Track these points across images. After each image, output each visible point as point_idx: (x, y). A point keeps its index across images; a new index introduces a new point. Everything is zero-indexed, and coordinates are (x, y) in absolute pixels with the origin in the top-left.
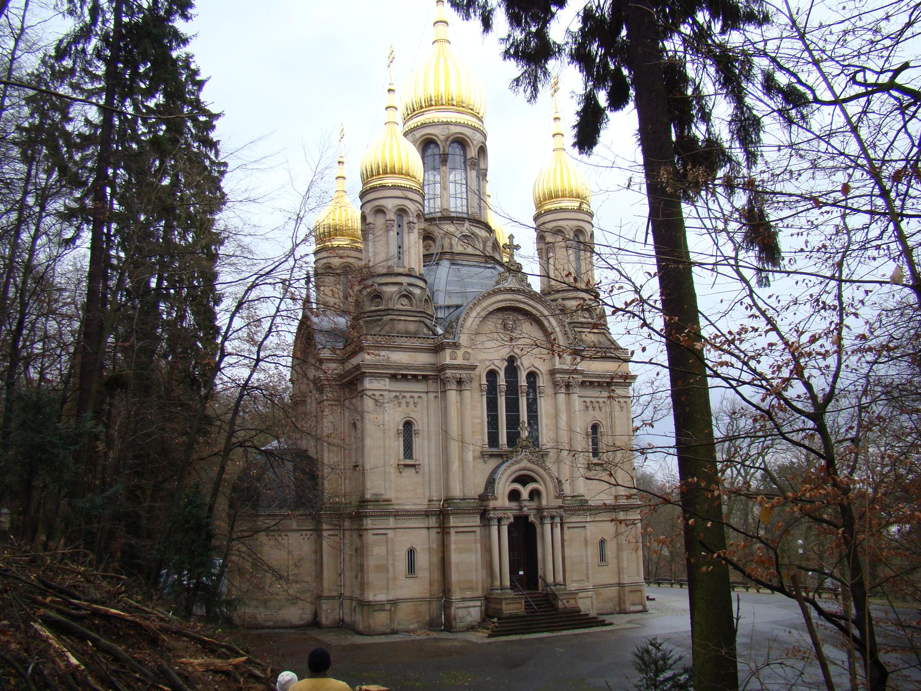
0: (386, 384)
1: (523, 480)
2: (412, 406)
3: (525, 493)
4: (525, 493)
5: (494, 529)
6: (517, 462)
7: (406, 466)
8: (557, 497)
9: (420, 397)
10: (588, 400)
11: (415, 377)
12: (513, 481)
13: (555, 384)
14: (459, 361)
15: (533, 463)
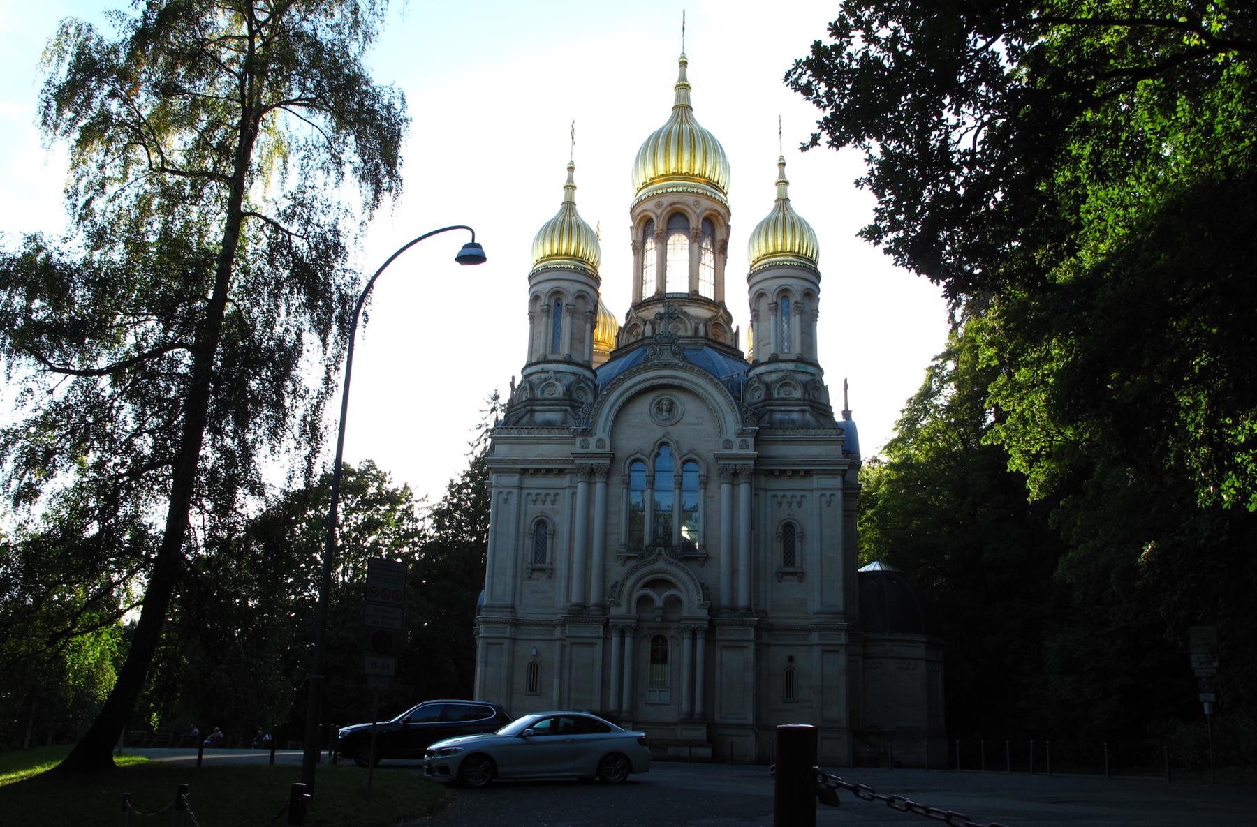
0: (514, 479)
1: (658, 583)
2: (548, 505)
3: (659, 602)
4: (659, 602)
5: (615, 641)
6: (650, 563)
7: (534, 570)
8: (701, 606)
9: (556, 494)
10: (780, 494)
11: (549, 471)
12: (645, 586)
13: (723, 471)
14: (593, 448)
15: (670, 563)
